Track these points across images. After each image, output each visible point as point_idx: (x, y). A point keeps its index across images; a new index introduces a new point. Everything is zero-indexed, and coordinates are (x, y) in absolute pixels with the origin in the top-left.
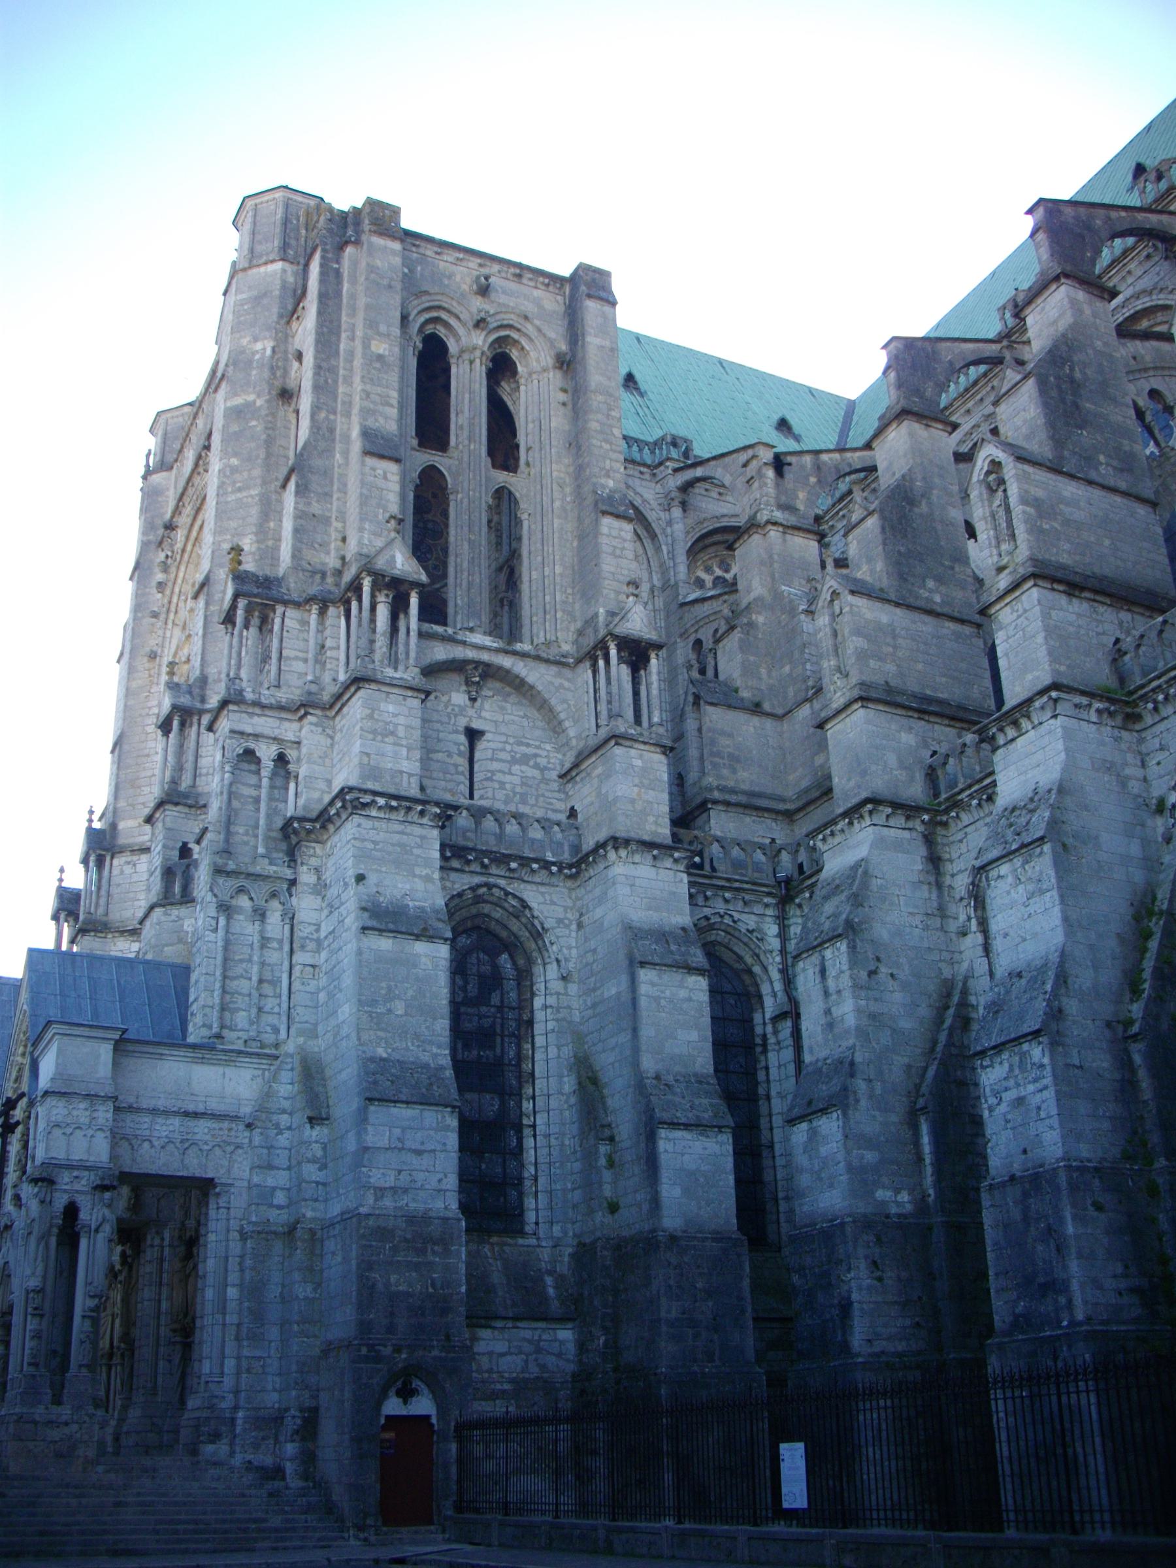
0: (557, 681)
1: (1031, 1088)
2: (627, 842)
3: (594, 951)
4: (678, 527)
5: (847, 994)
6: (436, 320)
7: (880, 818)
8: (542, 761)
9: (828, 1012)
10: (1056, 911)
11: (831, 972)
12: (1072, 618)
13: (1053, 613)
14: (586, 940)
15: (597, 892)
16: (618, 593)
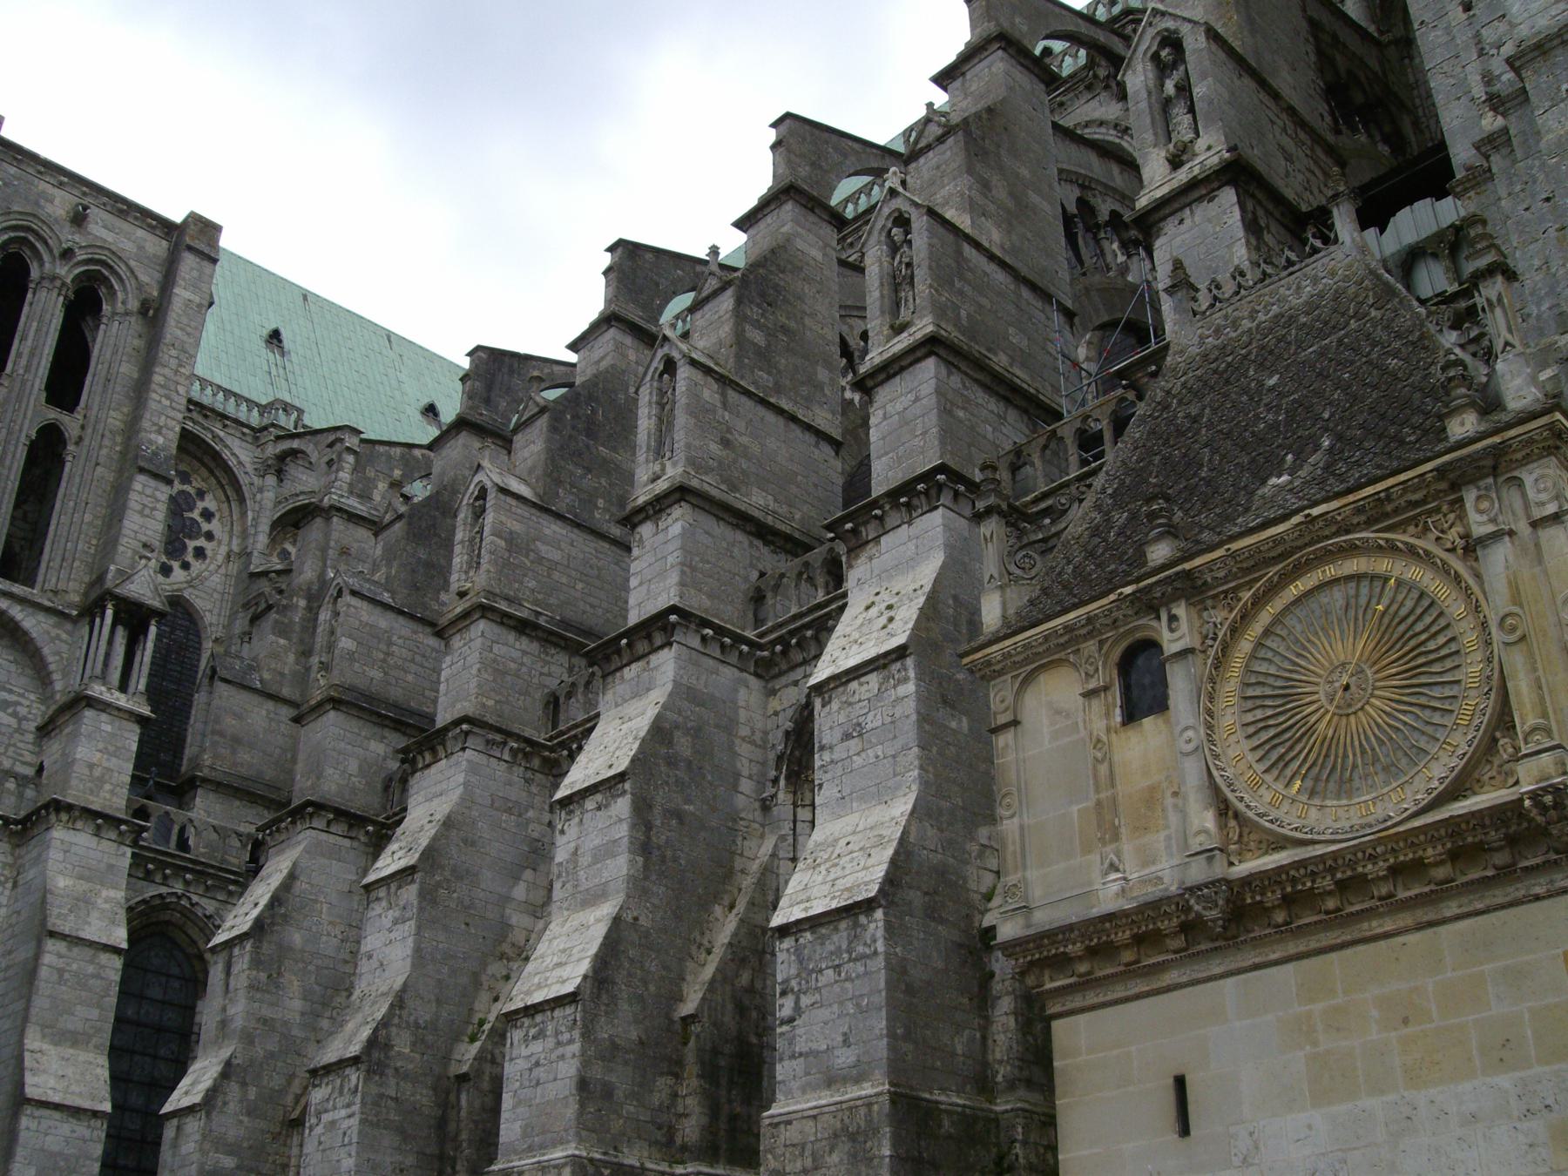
0: (54, 632)
1: (343, 1113)
2: (70, 808)
3: (18, 913)
4: (269, 496)
5: (241, 993)
6: (24, 241)
7: (319, 823)
8: (23, 711)
9: (224, 1009)
10: (410, 942)
11: (235, 969)
12: (516, 654)
13: (496, 648)
14: (16, 900)
15: (34, 854)
16: (135, 552)
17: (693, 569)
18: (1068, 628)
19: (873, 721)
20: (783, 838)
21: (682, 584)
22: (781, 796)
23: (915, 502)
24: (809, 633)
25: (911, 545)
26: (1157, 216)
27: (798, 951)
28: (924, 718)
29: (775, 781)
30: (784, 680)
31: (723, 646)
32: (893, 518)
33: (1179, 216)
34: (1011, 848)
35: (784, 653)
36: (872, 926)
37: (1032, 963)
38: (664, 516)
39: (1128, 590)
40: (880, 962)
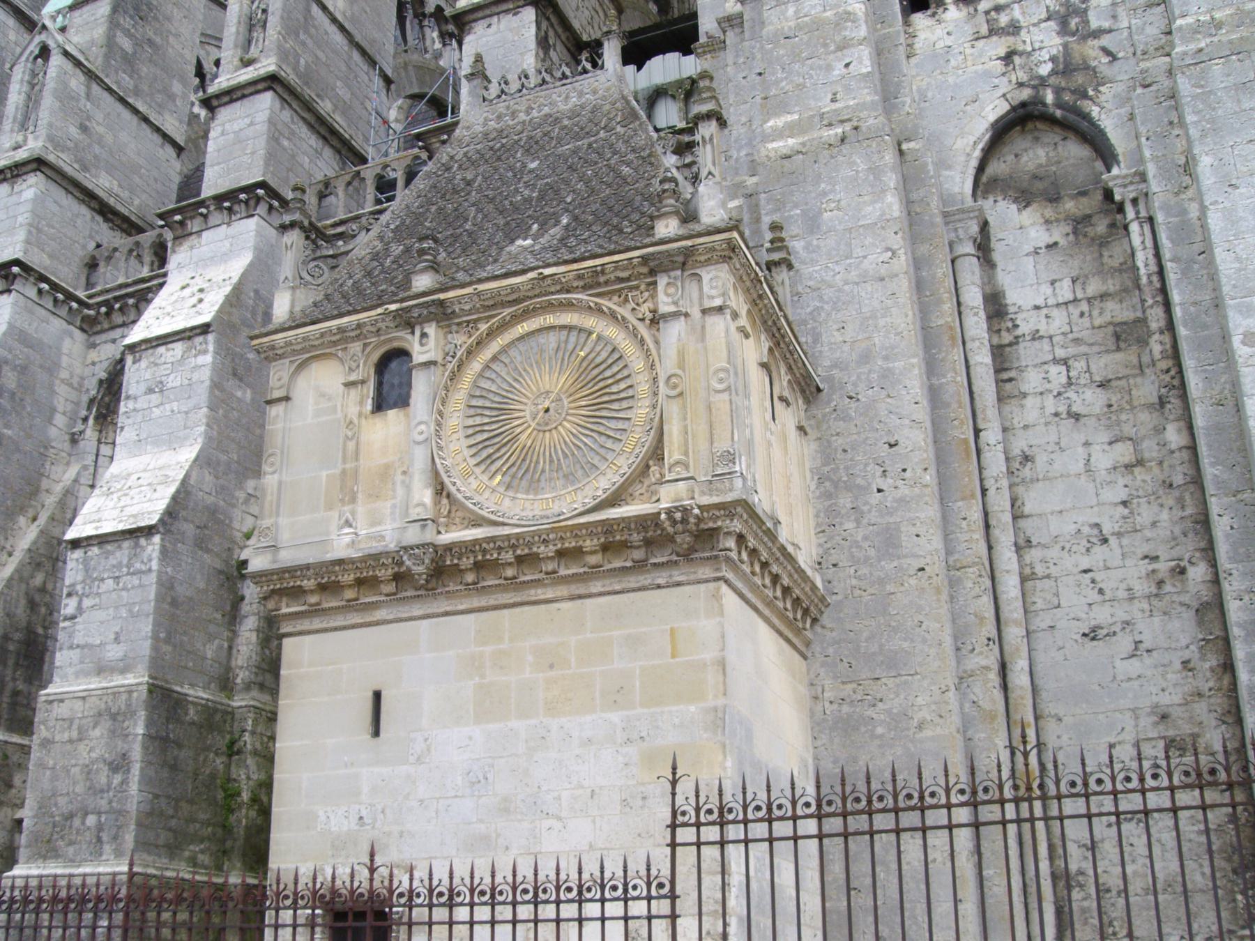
17: (39, 230)
18: (341, 330)
19: (173, 381)
20: (85, 468)
21: (28, 242)
22: (89, 432)
23: (236, 208)
24: (131, 301)
25: (227, 244)
26: (472, 17)
27: (86, 562)
28: (216, 385)
29: (85, 420)
30: (104, 337)
31: (56, 300)
32: (216, 218)
33: (487, 21)
34: (269, 498)
35: (108, 314)
36: (150, 548)
37: (273, 591)
38: (20, 180)
39: (393, 307)
40: (153, 577)
